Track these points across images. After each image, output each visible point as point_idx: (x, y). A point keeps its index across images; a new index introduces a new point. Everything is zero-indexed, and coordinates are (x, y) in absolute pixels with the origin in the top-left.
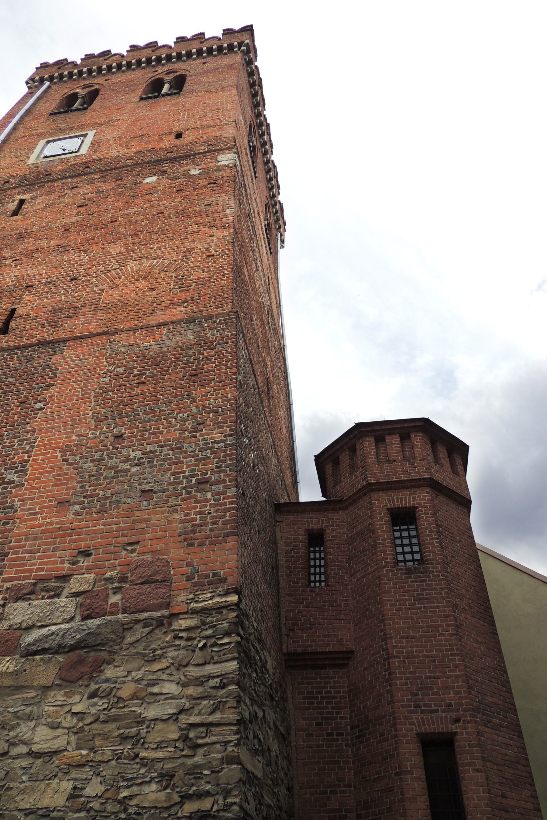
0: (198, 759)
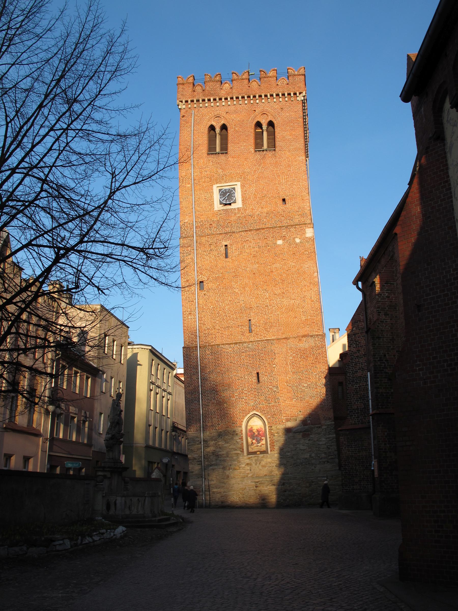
0: (330, 450)
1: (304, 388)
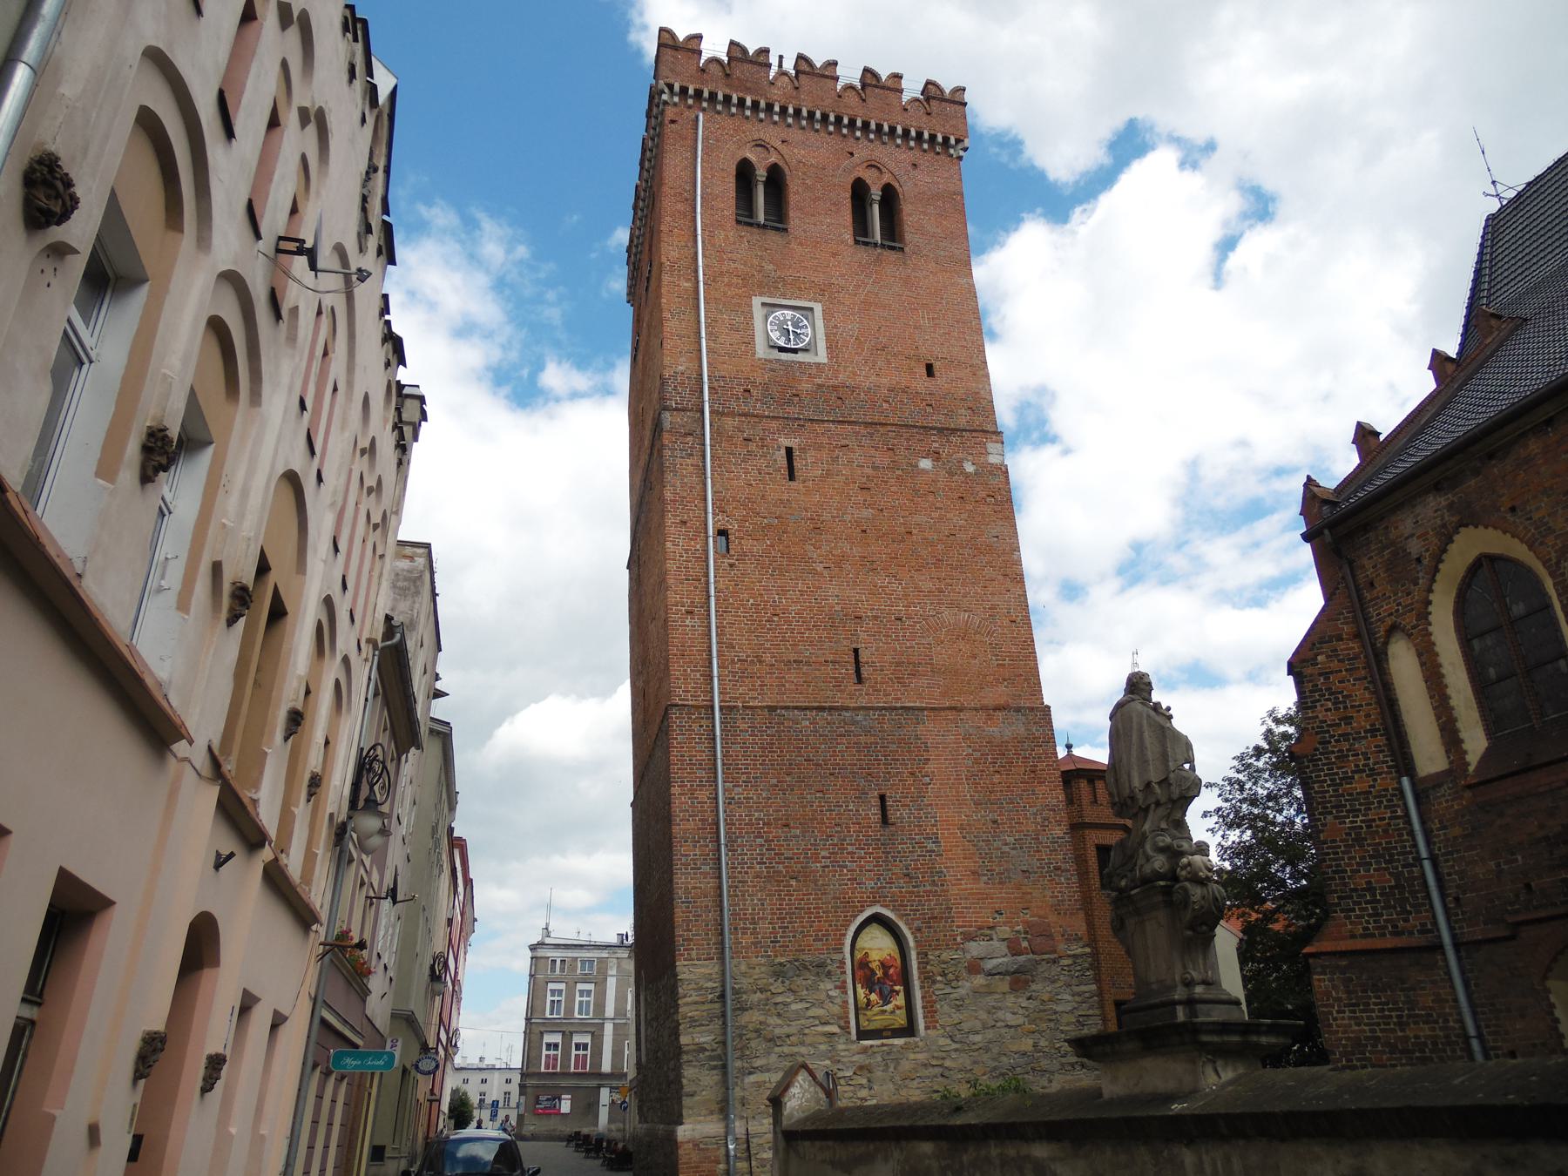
1: (1006, 848)
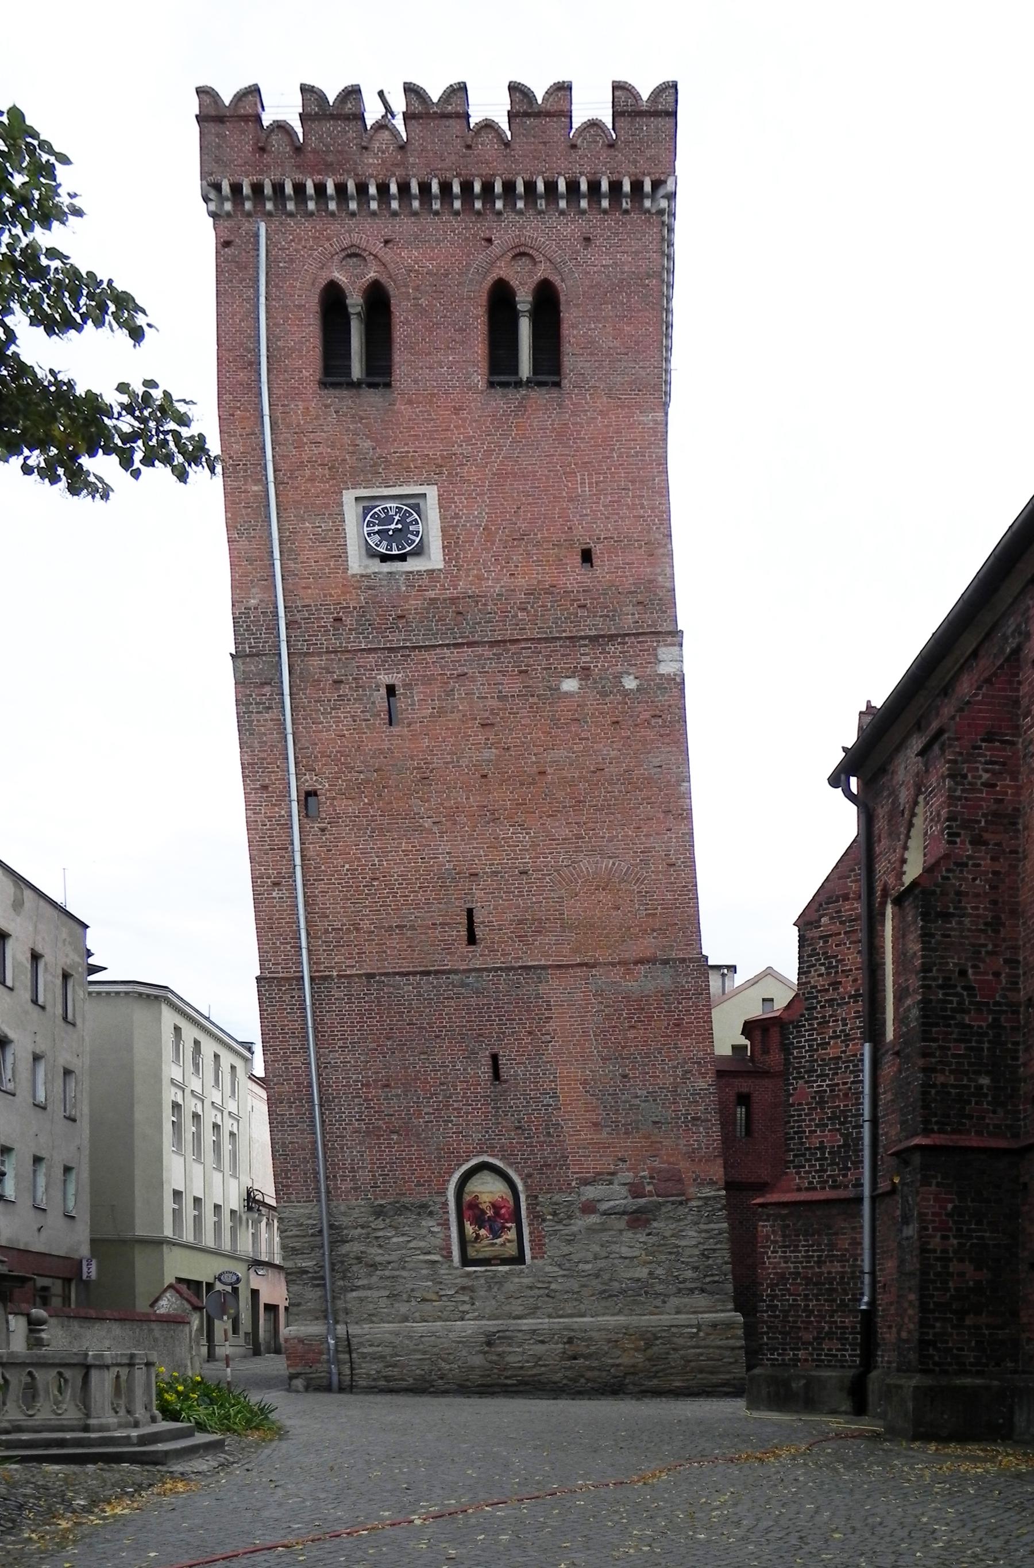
1: (637, 1101)
